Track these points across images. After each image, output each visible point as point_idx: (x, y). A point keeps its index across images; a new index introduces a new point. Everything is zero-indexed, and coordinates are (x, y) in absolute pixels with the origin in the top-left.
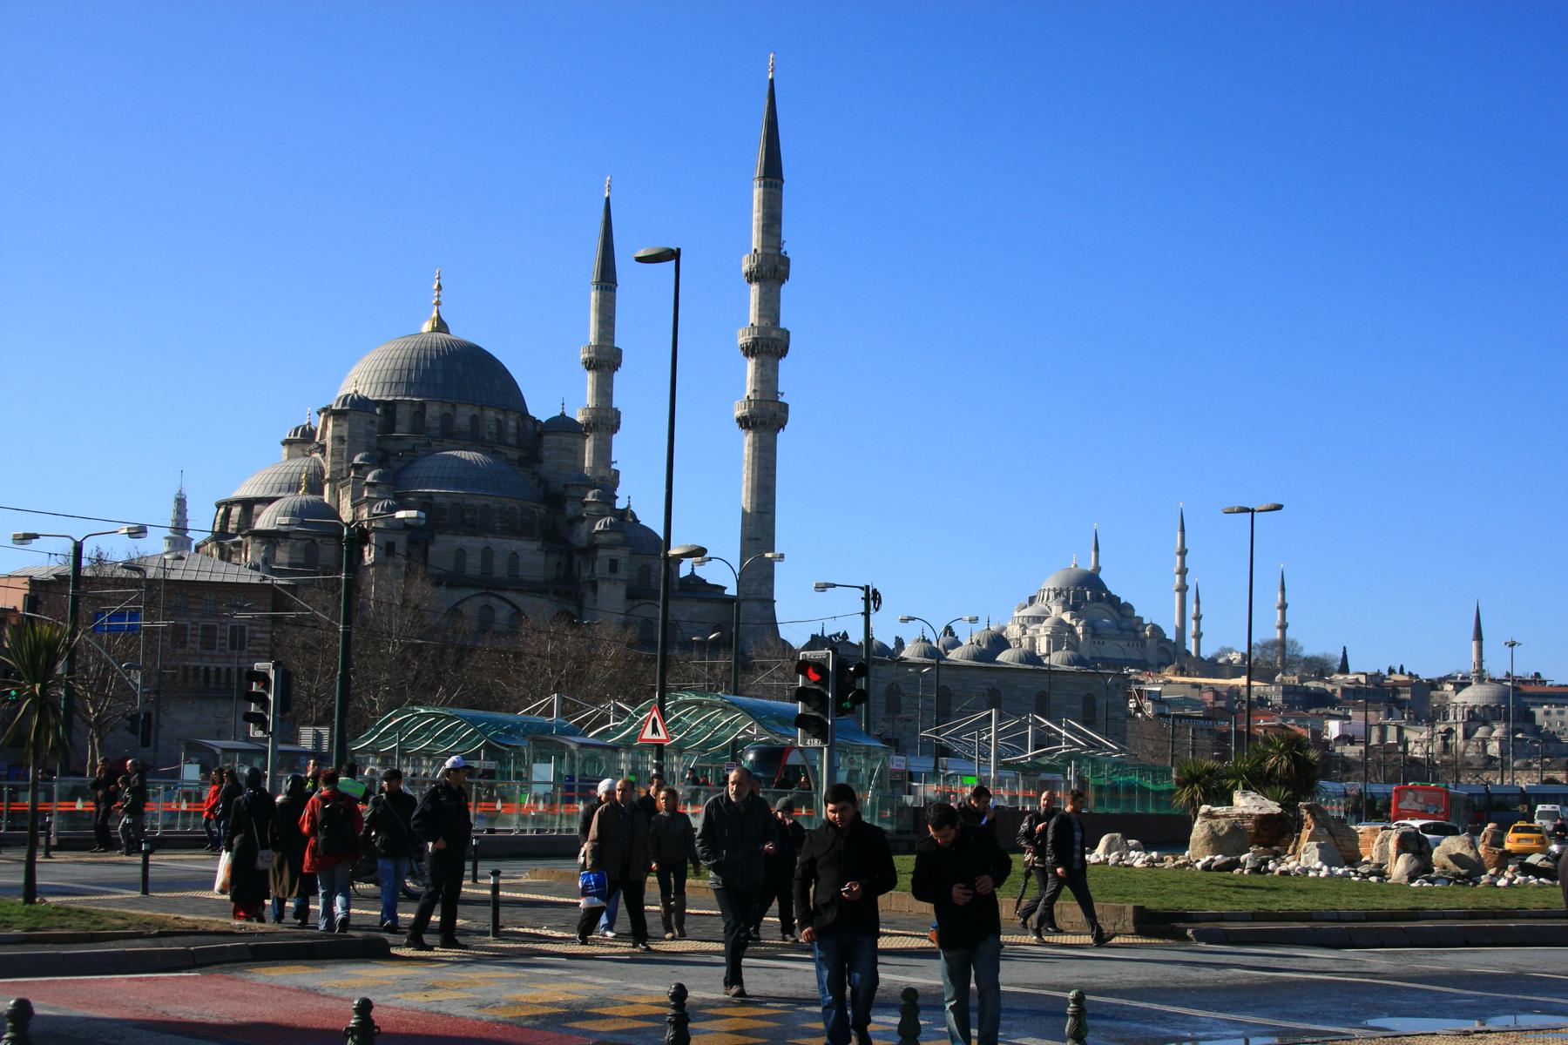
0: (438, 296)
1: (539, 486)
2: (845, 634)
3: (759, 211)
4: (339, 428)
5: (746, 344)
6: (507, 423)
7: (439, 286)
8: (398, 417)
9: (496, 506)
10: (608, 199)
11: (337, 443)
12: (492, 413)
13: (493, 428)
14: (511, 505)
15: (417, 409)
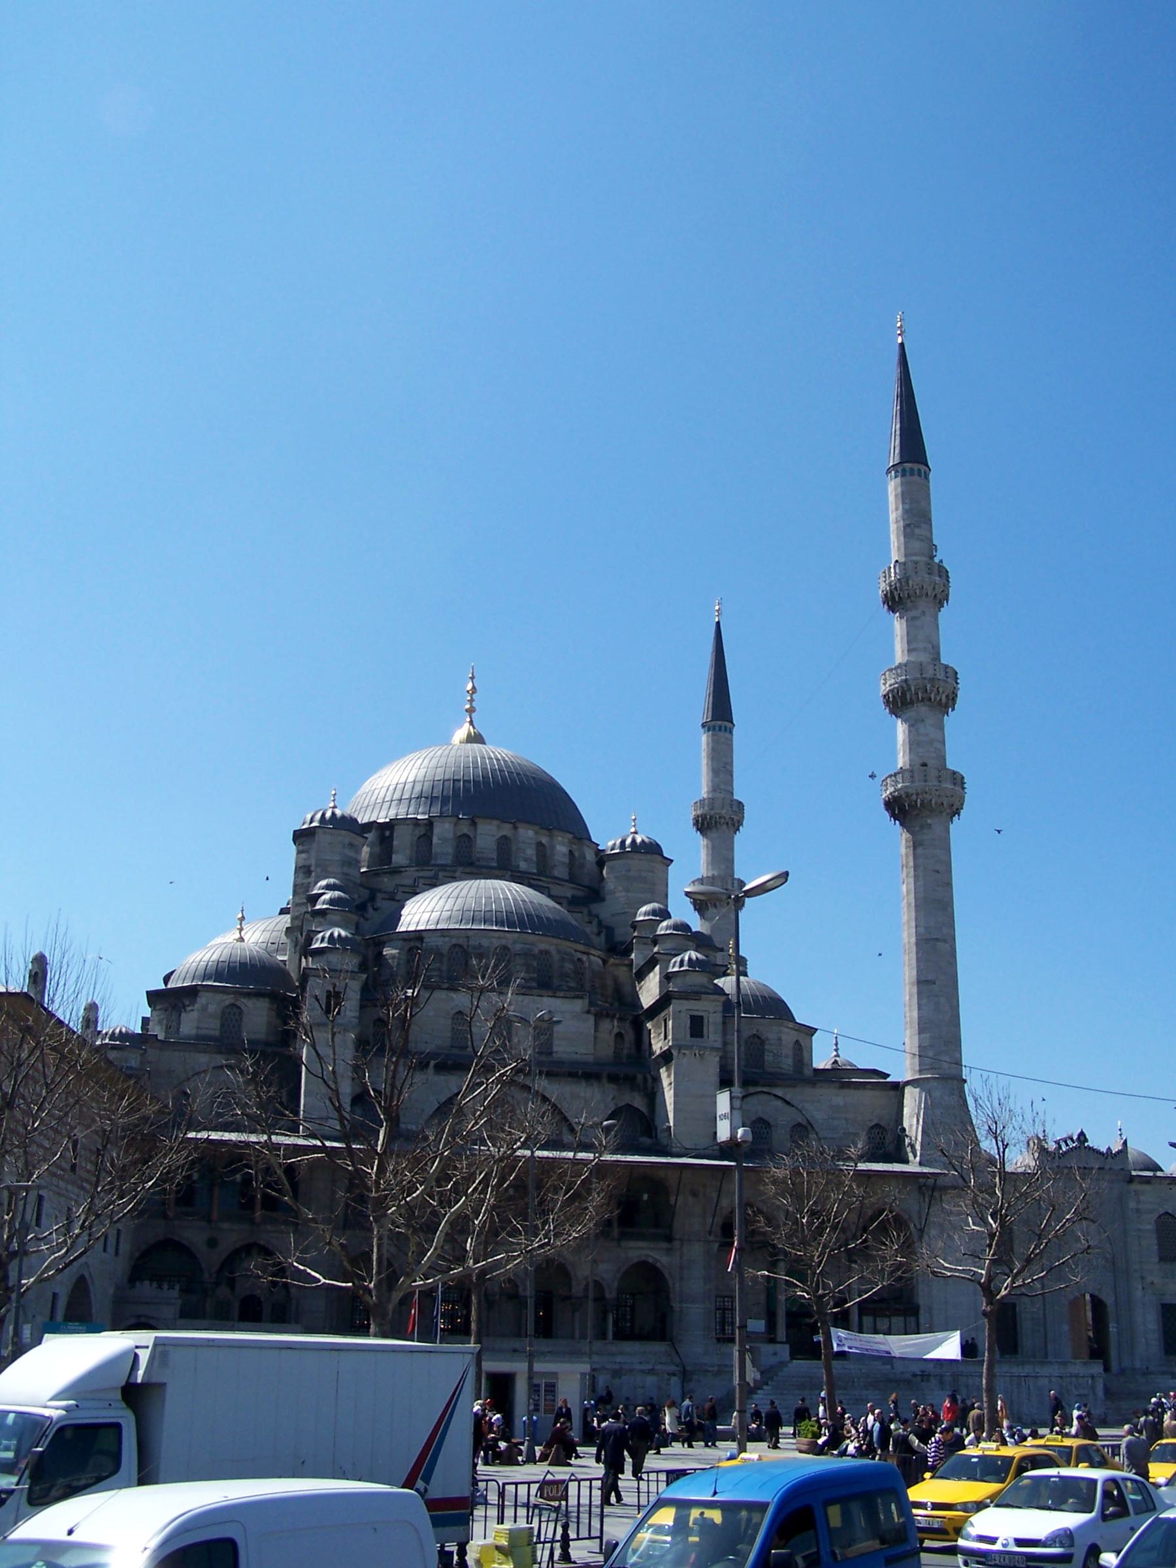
0: (471, 701)
1: (599, 934)
2: (1082, 1134)
3: (897, 509)
4: (303, 855)
5: (891, 691)
6: (553, 847)
7: (474, 687)
8: (395, 843)
9: (518, 947)
10: (718, 623)
11: (301, 875)
12: (531, 833)
13: (531, 852)
14: (543, 946)
15: (421, 831)
